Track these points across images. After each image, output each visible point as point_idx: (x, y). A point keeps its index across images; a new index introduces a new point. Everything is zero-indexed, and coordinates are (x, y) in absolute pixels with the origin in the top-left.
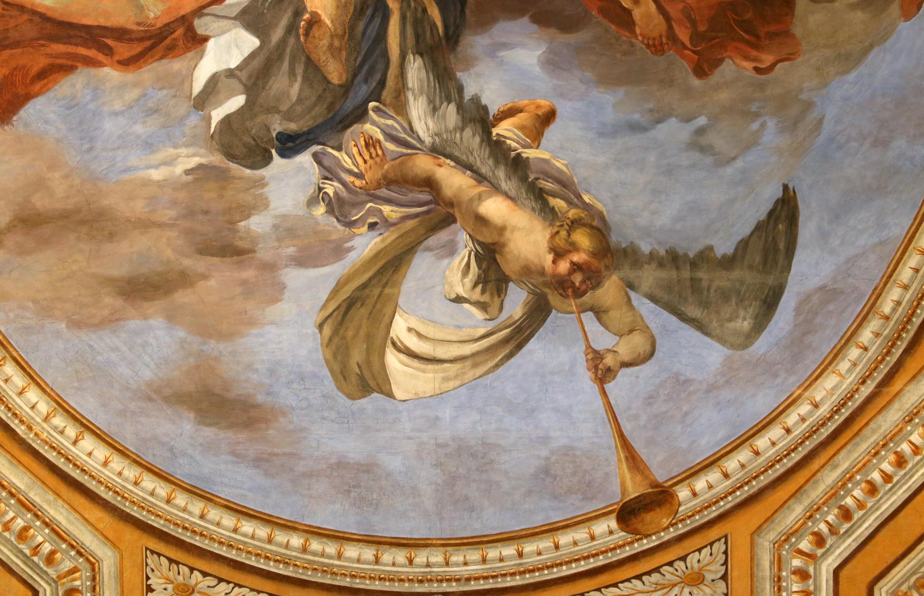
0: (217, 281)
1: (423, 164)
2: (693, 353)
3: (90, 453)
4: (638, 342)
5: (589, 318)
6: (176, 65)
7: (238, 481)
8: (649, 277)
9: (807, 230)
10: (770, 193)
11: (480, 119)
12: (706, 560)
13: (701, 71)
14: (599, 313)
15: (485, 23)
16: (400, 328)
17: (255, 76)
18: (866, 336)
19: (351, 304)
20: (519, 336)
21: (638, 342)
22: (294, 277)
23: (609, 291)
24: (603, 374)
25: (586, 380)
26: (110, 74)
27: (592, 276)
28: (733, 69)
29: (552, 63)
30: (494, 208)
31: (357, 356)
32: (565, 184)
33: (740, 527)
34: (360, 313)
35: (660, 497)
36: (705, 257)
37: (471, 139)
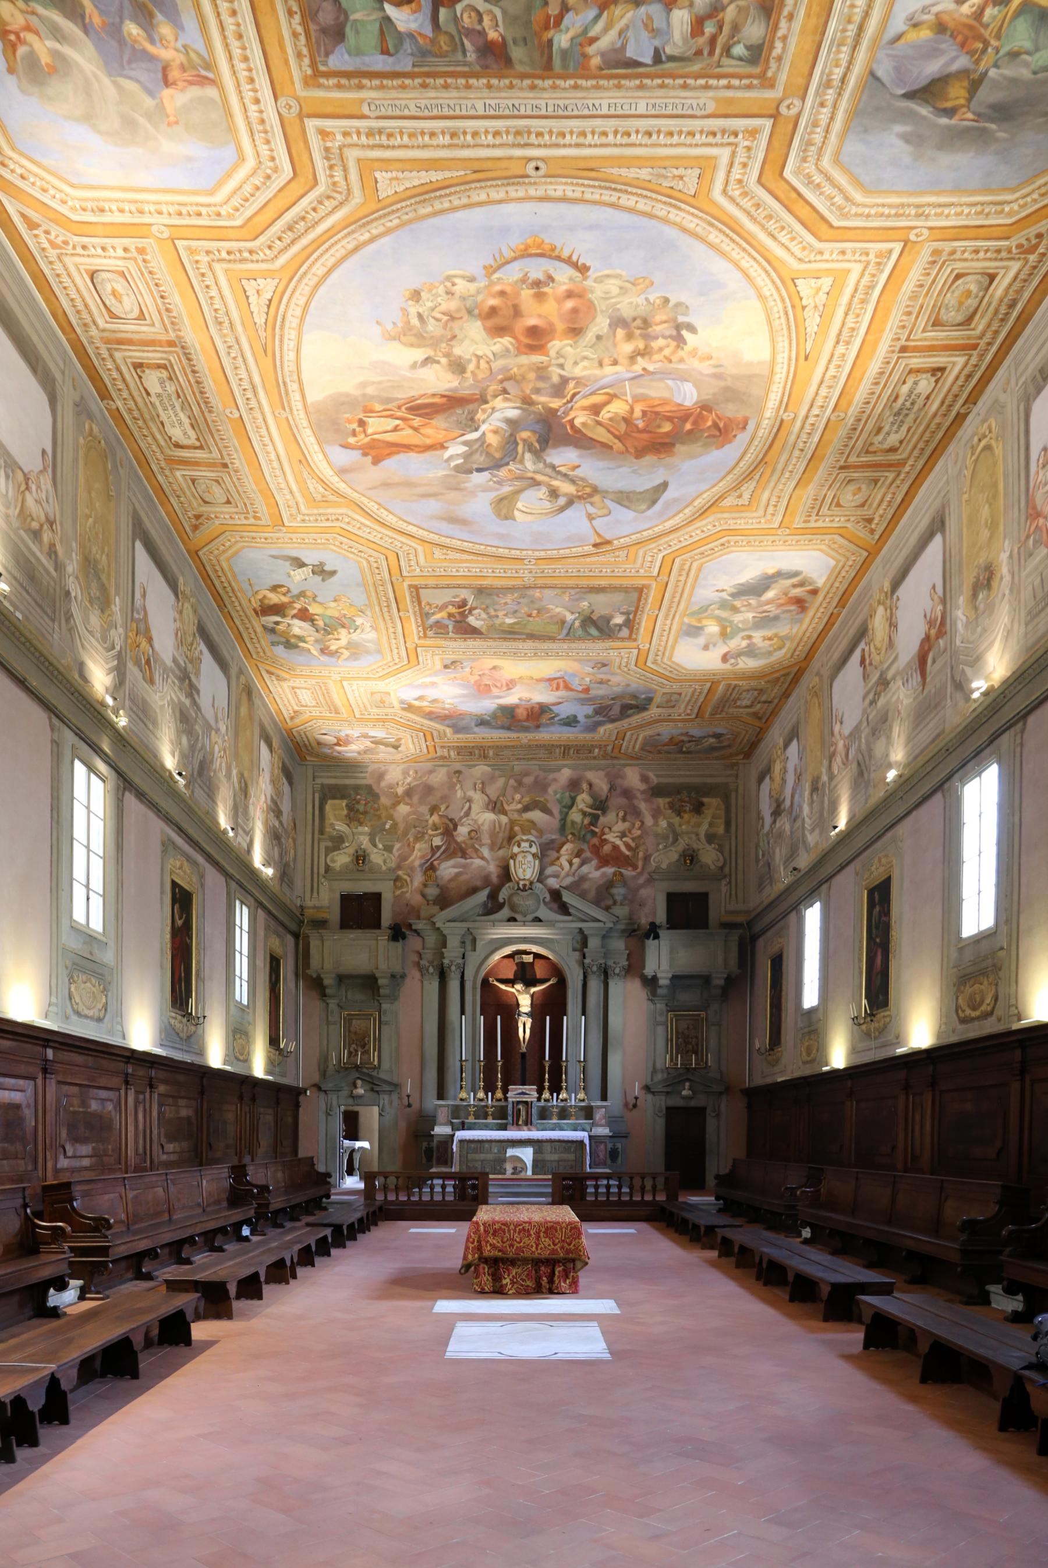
0: (452, 495)
1: (530, 475)
2: (624, 514)
3: (412, 529)
4: (605, 511)
5: (588, 506)
6: (437, 453)
7: (464, 535)
8: (611, 496)
9: (670, 488)
10: (659, 481)
11: (553, 467)
12: (622, 554)
13: (637, 458)
14: (592, 504)
15: (555, 446)
16: (519, 505)
17: (467, 456)
18: (687, 511)
19: (502, 499)
20: (562, 509)
21: (605, 511)
22: (481, 495)
23: (596, 499)
24: (591, 518)
25: (586, 522)
26: (412, 455)
27: (590, 495)
28: (649, 459)
29: (580, 456)
30: (555, 483)
31: (504, 511)
32: (582, 479)
33: (633, 549)
34: (505, 502)
35: (608, 542)
36: (634, 492)
37: (549, 471)
